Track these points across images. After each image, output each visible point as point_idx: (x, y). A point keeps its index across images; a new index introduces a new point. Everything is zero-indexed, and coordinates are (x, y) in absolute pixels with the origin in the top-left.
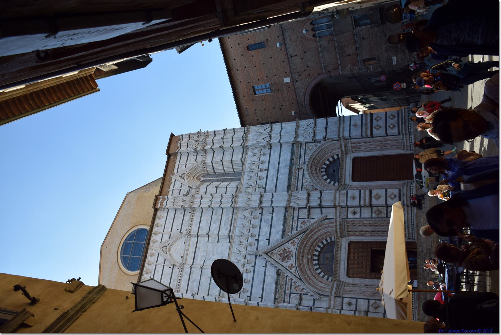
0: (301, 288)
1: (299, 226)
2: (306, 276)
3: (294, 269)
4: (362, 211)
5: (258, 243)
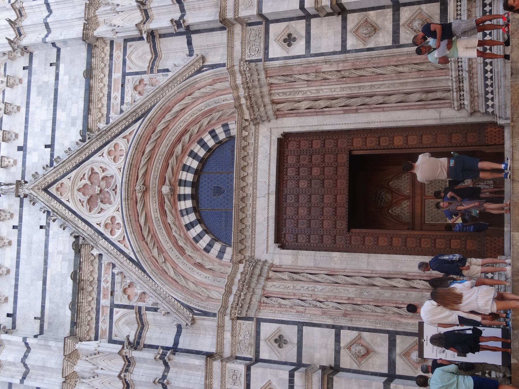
0: (138, 290)
1: (128, 99)
2: (155, 252)
3: (119, 232)
4: (313, 32)
5: (24, 157)
